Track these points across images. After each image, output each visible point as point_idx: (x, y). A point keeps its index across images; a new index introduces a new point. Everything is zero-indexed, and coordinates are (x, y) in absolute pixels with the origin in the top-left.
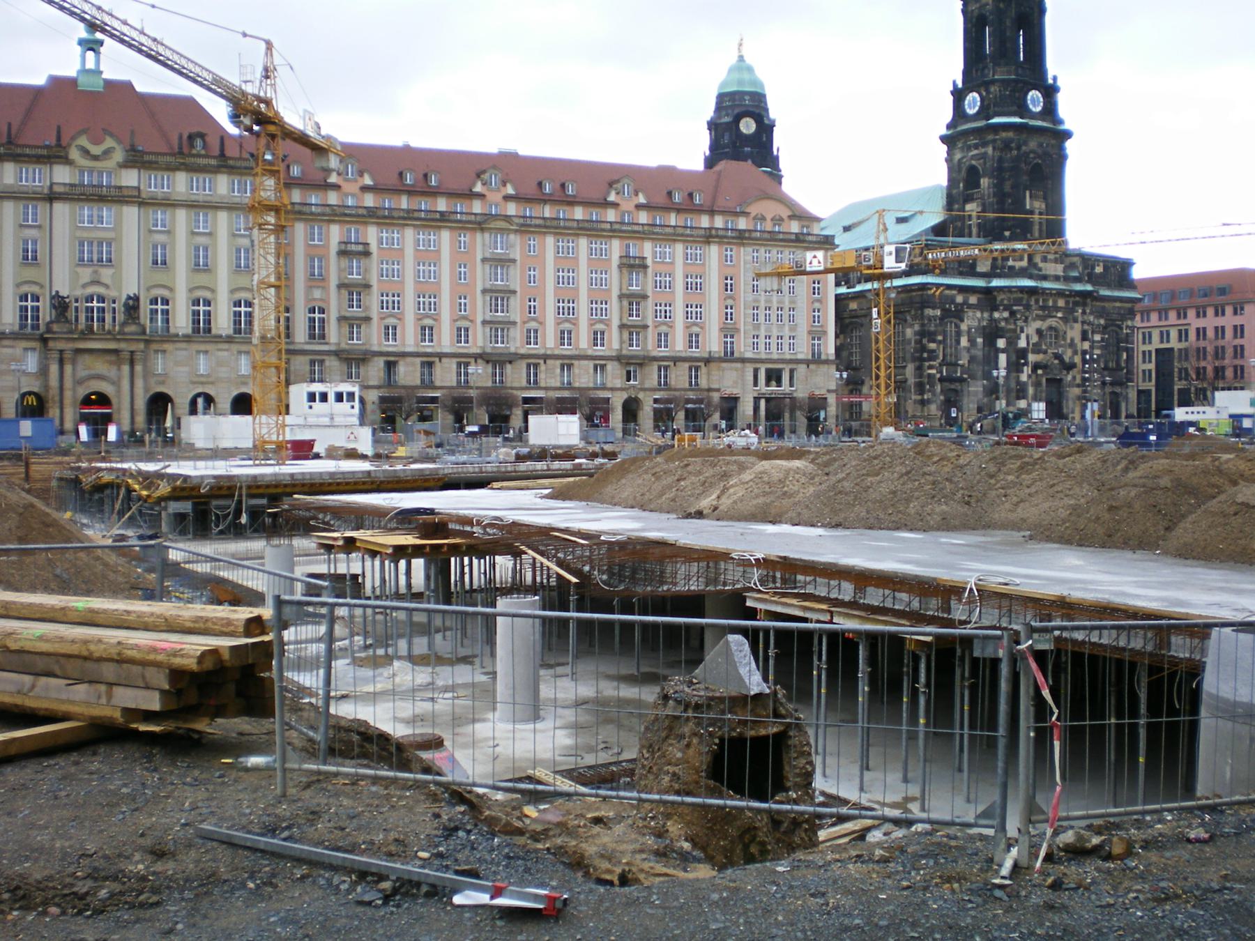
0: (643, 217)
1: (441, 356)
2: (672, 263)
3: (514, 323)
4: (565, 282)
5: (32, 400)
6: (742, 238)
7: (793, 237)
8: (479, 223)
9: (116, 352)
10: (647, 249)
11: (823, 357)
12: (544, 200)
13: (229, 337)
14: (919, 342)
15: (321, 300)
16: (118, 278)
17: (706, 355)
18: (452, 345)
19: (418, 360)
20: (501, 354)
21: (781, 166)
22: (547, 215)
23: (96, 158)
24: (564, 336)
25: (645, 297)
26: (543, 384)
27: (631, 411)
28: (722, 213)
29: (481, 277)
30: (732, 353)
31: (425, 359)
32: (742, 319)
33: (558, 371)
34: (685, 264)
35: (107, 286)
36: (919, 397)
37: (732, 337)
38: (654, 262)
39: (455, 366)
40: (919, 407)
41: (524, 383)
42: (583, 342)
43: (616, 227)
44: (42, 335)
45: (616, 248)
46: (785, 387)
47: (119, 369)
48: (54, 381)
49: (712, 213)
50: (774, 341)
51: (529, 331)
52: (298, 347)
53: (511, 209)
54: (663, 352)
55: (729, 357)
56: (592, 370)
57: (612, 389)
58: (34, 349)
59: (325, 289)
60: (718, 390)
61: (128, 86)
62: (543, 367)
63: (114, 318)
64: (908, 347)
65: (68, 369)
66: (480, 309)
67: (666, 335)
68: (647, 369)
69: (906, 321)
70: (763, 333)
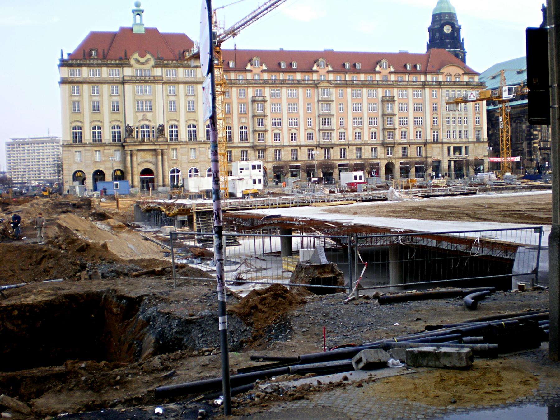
0: (393, 77)
2: (407, 98)
3: (334, 130)
5: (118, 173)
6: (440, 85)
7: (465, 83)
8: (316, 84)
9: (155, 150)
10: (395, 92)
11: (482, 140)
12: (346, 72)
13: (204, 141)
14: (529, 131)
15: (246, 123)
16: (155, 117)
17: (424, 141)
19: (290, 149)
21: (466, 47)
22: (347, 79)
23: (142, 64)
24: (358, 135)
25: (394, 115)
26: (347, 158)
27: (389, 168)
28: (431, 73)
29: (317, 109)
30: (437, 140)
31: (293, 148)
32: (442, 122)
33: (355, 151)
34: (413, 98)
35: (150, 121)
36: (529, 158)
37: (437, 132)
38: (398, 98)
39: (307, 151)
40: (530, 162)
41: (339, 157)
43: (380, 83)
44: (122, 144)
45: (380, 92)
46: (464, 155)
47: (157, 158)
48: (129, 165)
49: (425, 74)
50: (457, 133)
51: (340, 133)
52: (235, 145)
53: (331, 77)
54: (404, 140)
55: (436, 141)
56: (370, 150)
57: (380, 159)
58: (119, 150)
60: (430, 157)
61: (155, 30)
62: (347, 150)
63: (154, 135)
64: (523, 134)
65: (135, 158)
66: (317, 124)
68: (396, 149)
69: (522, 121)
70: (451, 130)
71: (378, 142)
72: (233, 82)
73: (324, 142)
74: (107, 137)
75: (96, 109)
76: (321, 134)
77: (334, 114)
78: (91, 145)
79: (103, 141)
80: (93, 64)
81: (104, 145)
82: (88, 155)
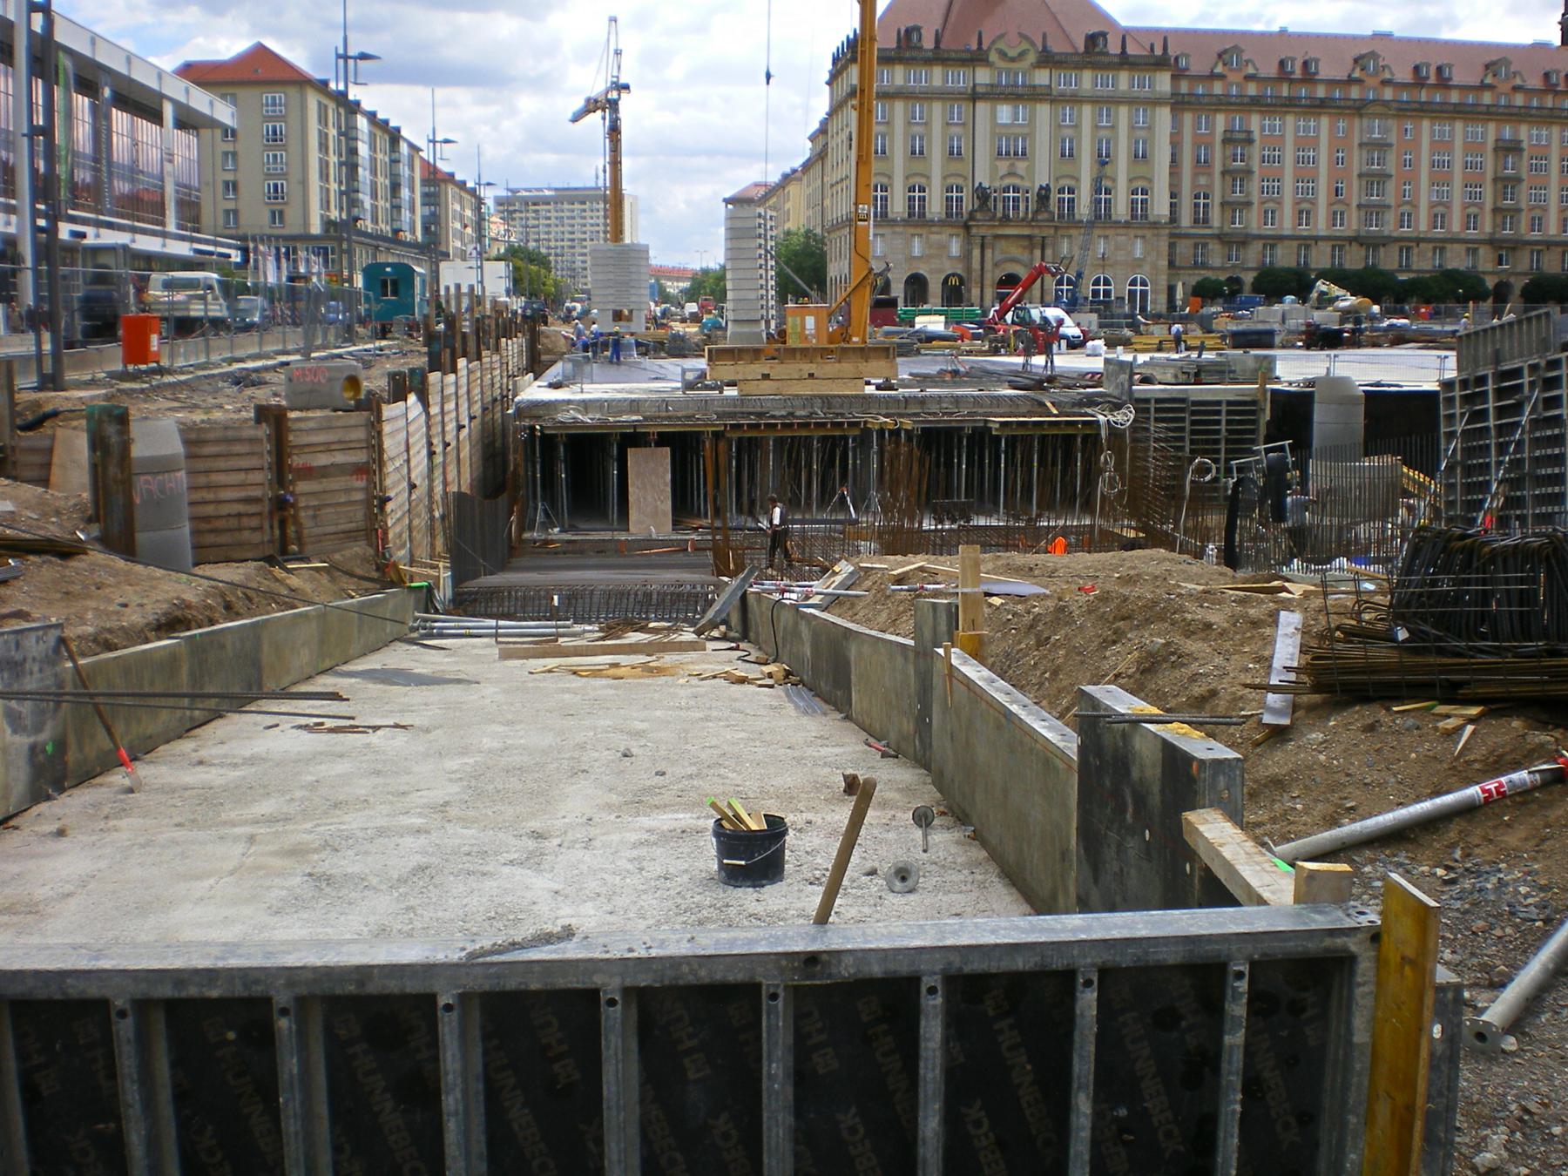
1: (1317, 239)
3: (1389, 207)
5: (954, 281)
8: (1359, 109)
9: (1030, 237)
18: (1328, 228)
19: (1295, 243)
20: (1375, 238)
24: (1437, 219)
33: (1430, 254)
35: (1022, 178)
39: (1329, 249)
42: (1456, 226)
44: (966, 223)
47: (1032, 253)
48: (976, 265)
57: (1484, 273)
58: (958, 235)
59: (1210, 175)
62: (1415, 251)
65: (988, 253)
66: (1354, 193)
71: (1482, 237)
72: (1186, 99)
73: (1368, 231)
74: (935, 208)
75: (917, 154)
76: (1363, 213)
77: (1393, 172)
81: (931, 223)
82: (899, 242)
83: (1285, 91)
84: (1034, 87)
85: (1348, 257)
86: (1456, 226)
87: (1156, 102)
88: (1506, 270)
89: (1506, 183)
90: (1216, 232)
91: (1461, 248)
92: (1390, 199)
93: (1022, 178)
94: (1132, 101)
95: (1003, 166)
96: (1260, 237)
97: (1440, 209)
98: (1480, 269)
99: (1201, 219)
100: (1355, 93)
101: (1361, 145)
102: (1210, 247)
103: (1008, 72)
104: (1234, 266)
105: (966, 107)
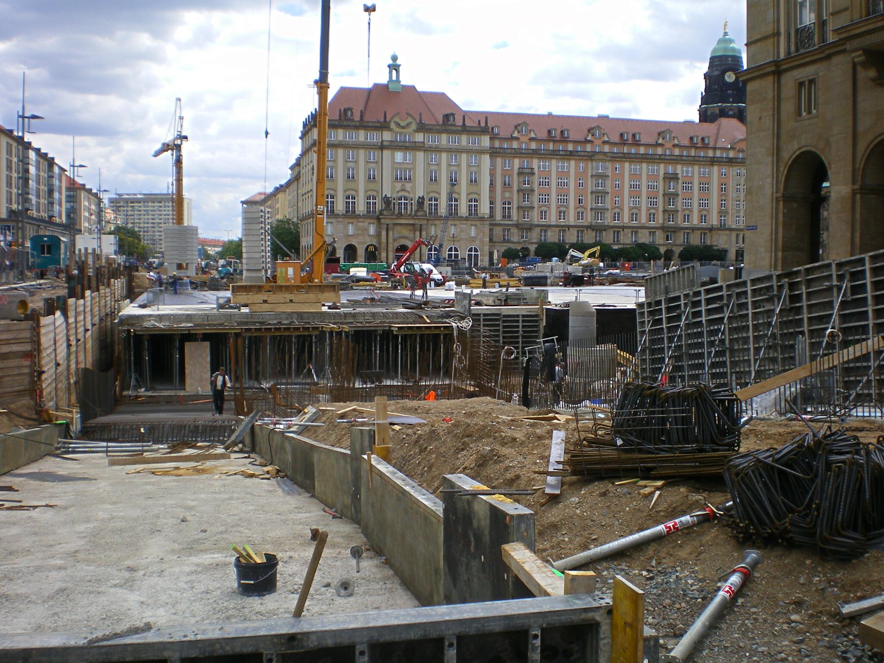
1: (569, 227)
4: (635, 189)
5: (372, 249)
8: (591, 157)
9: (413, 225)
13: (466, 217)
18: (575, 221)
19: (557, 229)
20: (601, 226)
24: (634, 216)
33: (630, 235)
35: (409, 192)
38: (683, 176)
41: (612, 241)
44: (378, 216)
47: (414, 234)
48: (384, 240)
52: (497, 222)
56: (648, 235)
57: (659, 245)
58: (373, 223)
59: (511, 192)
62: (622, 233)
65: (391, 233)
66: (589, 202)
67: (688, 216)
74: (361, 208)
75: (350, 178)
78: (344, 216)
79: (357, 212)
80: (349, 126)
81: (358, 217)
82: (341, 226)
83: (551, 146)
84: (415, 142)
85: (586, 236)
86: (644, 220)
87: (482, 152)
88: (670, 243)
89: (670, 197)
90: (515, 223)
91: (647, 231)
92: (608, 205)
93: (409, 192)
94: (469, 151)
95: (399, 186)
96: (538, 226)
97: (635, 211)
98: (657, 243)
99: (506, 216)
100: (589, 148)
101: (592, 176)
102: (512, 230)
103: (401, 134)
104: (525, 242)
105: (378, 153)
